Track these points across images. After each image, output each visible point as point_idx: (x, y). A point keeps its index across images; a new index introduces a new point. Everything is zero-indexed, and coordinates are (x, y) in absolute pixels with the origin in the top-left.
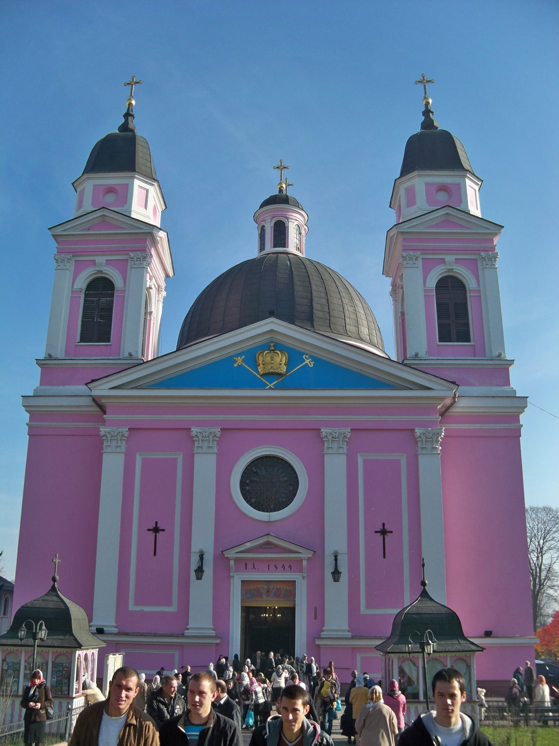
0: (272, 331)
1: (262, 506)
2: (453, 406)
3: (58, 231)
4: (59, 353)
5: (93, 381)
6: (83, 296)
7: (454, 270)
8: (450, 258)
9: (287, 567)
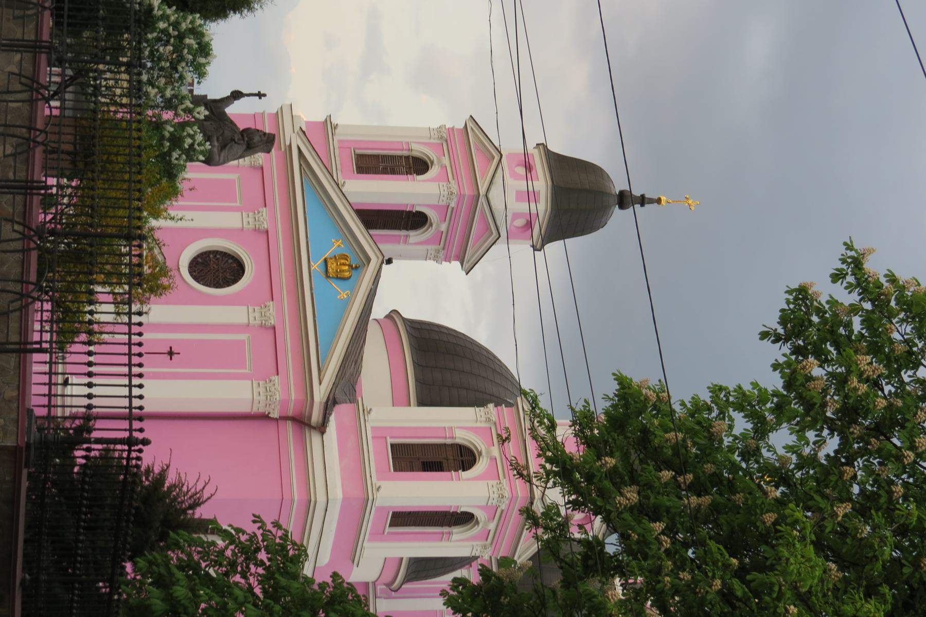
0: (369, 260)
1: (195, 266)
2: (312, 430)
3: (470, 125)
4: (340, 135)
6: (405, 153)
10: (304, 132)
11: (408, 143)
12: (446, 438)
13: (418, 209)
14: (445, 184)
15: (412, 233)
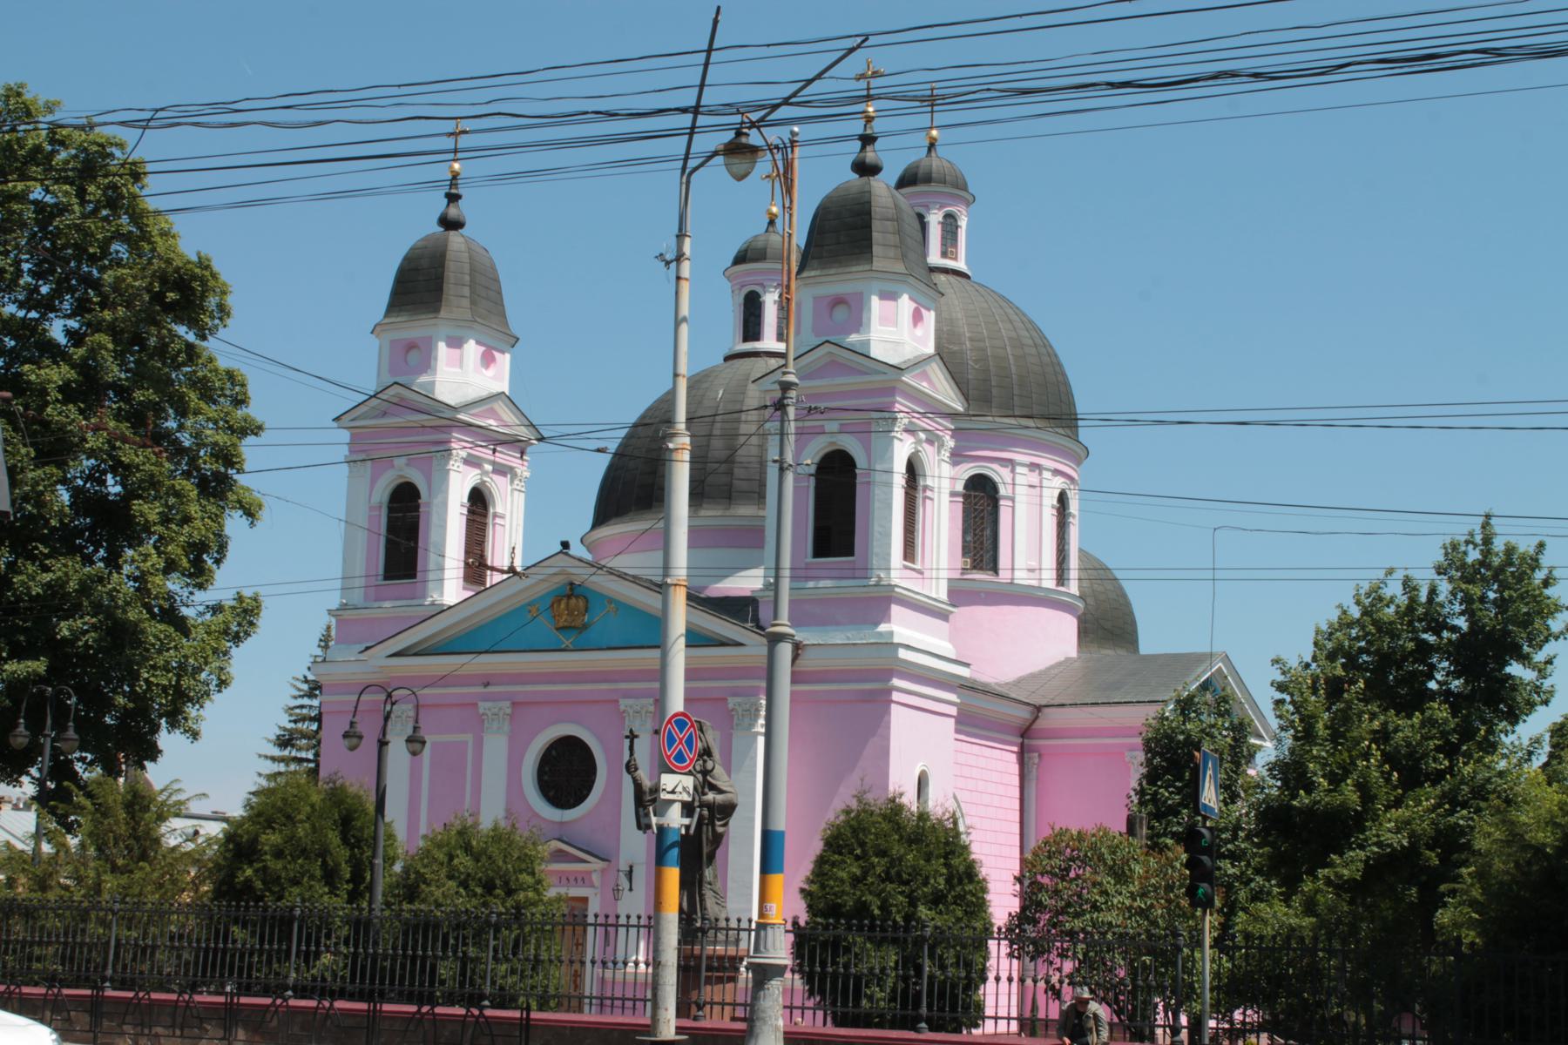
5: (367, 648)
6: (384, 512)
7: (839, 443)
8: (832, 426)
9: (572, 879)
10: (367, 648)
11: (371, 508)
12: (808, 487)
13: (465, 500)
14: (435, 462)
15: (491, 510)
